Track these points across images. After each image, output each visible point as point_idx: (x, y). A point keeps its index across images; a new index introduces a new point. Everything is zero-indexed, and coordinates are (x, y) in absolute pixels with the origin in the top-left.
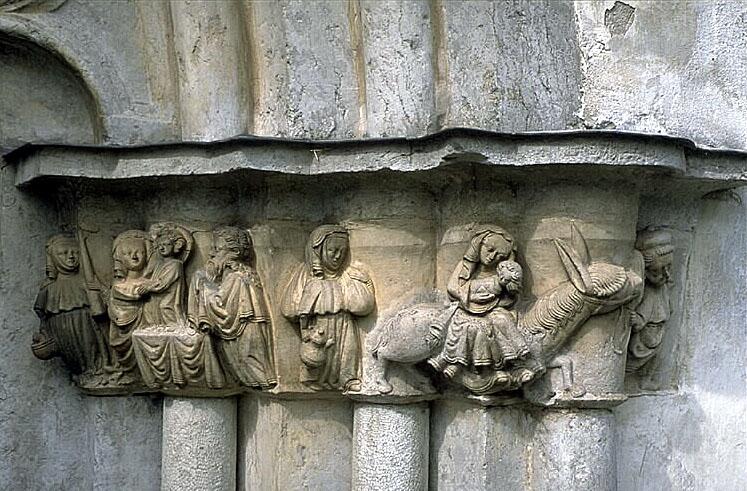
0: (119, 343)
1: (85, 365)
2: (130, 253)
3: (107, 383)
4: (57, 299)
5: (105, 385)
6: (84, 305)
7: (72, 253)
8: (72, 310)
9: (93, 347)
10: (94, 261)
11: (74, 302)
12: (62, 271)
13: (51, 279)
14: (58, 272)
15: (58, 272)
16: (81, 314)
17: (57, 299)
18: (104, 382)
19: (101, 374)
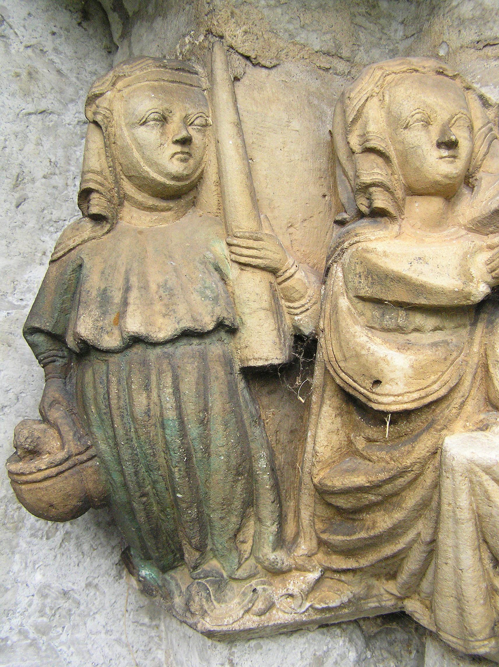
0: (360, 480)
1: (201, 548)
2: (427, 123)
3: (271, 606)
4: (117, 297)
5: (261, 613)
6: (220, 325)
7: (186, 122)
8: (173, 341)
9: (239, 488)
10: (258, 156)
11: (182, 309)
12: (140, 197)
13: (97, 219)
14: (123, 198)
15: (123, 198)
16: (203, 357)
17: (117, 297)
18: (260, 605)
19: (251, 576)
